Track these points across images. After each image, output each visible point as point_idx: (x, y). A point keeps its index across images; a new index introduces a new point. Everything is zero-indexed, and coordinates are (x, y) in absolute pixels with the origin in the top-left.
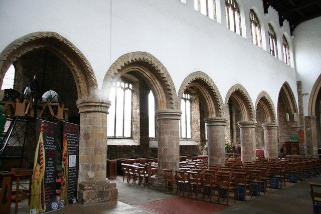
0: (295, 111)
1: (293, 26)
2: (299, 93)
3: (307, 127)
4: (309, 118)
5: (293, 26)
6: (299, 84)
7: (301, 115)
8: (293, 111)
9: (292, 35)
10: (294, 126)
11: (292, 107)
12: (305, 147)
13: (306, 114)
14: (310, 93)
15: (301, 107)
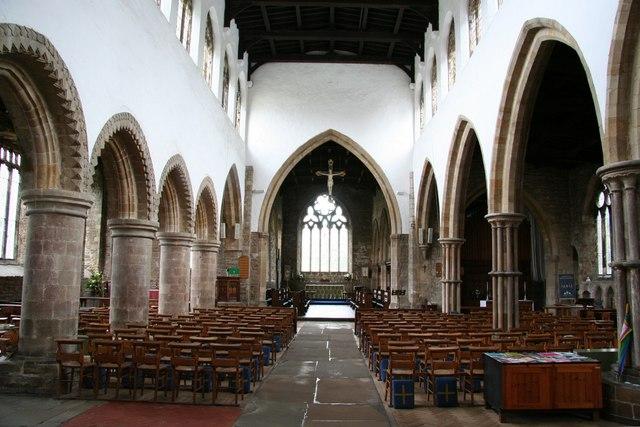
0: (238, 220)
1: (253, 64)
2: (248, 188)
3: (254, 251)
4: (259, 235)
5: (253, 64)
6: (249, 171)
7: (247, 228)
8: (233, 220)
9: (249, 79)
10: (233, 248)
11: (233, 212)
12: (248, 288)
13: (254, 227)
14: (265, 192)
15: (247, 215)
